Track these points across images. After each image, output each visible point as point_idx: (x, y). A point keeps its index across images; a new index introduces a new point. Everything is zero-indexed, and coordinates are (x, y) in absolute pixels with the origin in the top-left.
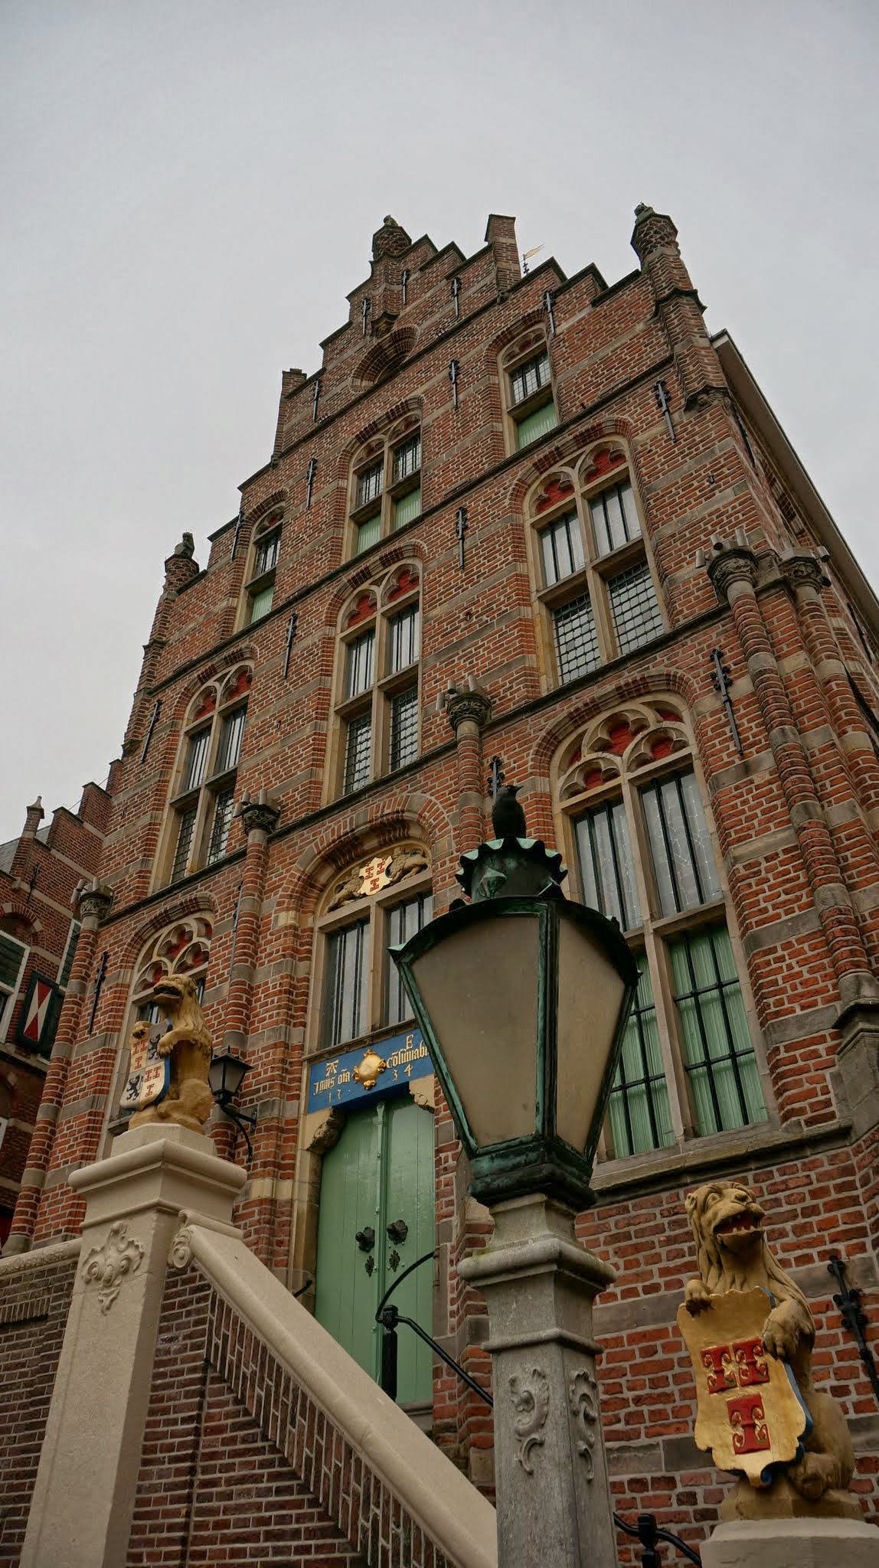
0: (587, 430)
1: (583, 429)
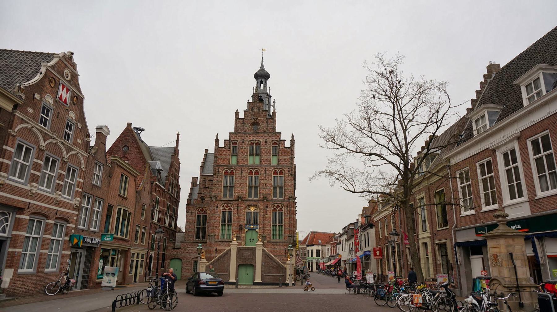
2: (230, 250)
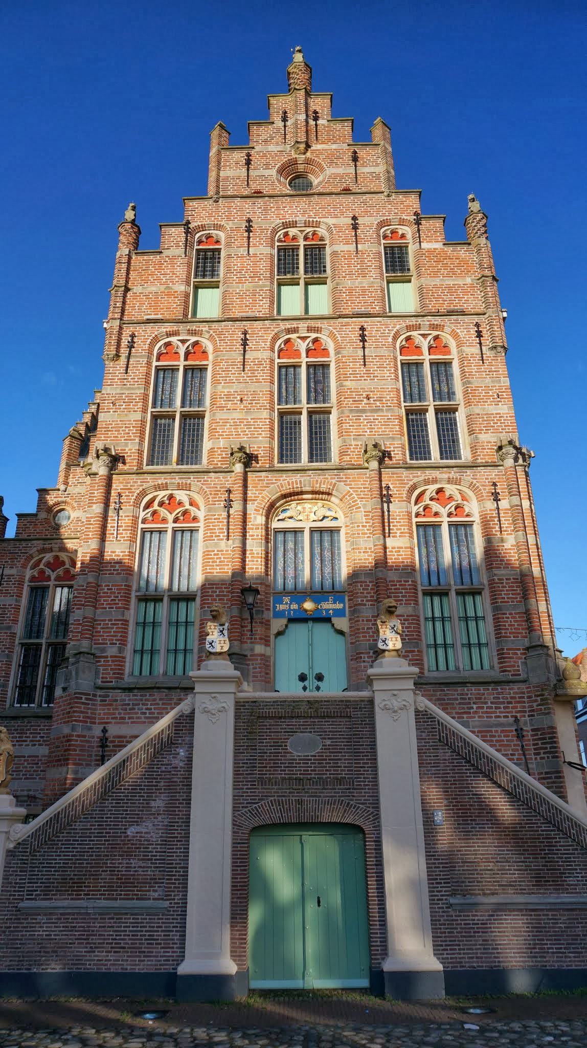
0: (437, 325)
1: (436, 323)
2: (185, 724)
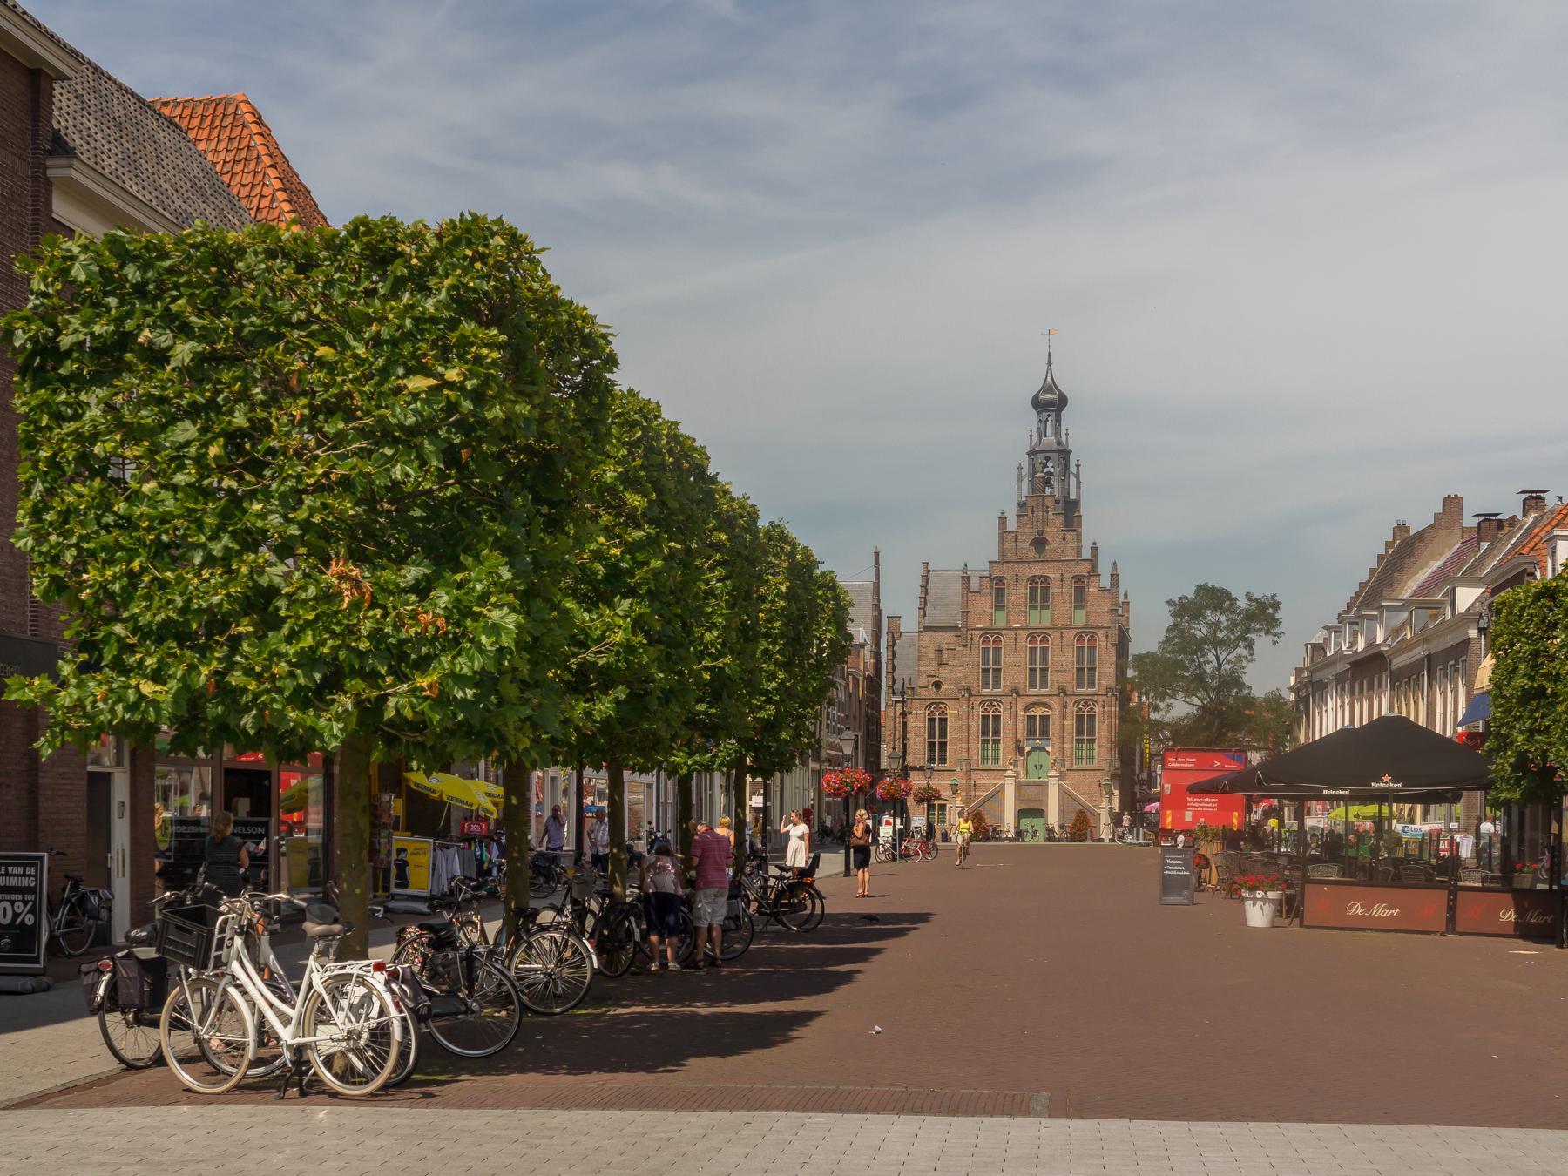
2: (1003, 786)
